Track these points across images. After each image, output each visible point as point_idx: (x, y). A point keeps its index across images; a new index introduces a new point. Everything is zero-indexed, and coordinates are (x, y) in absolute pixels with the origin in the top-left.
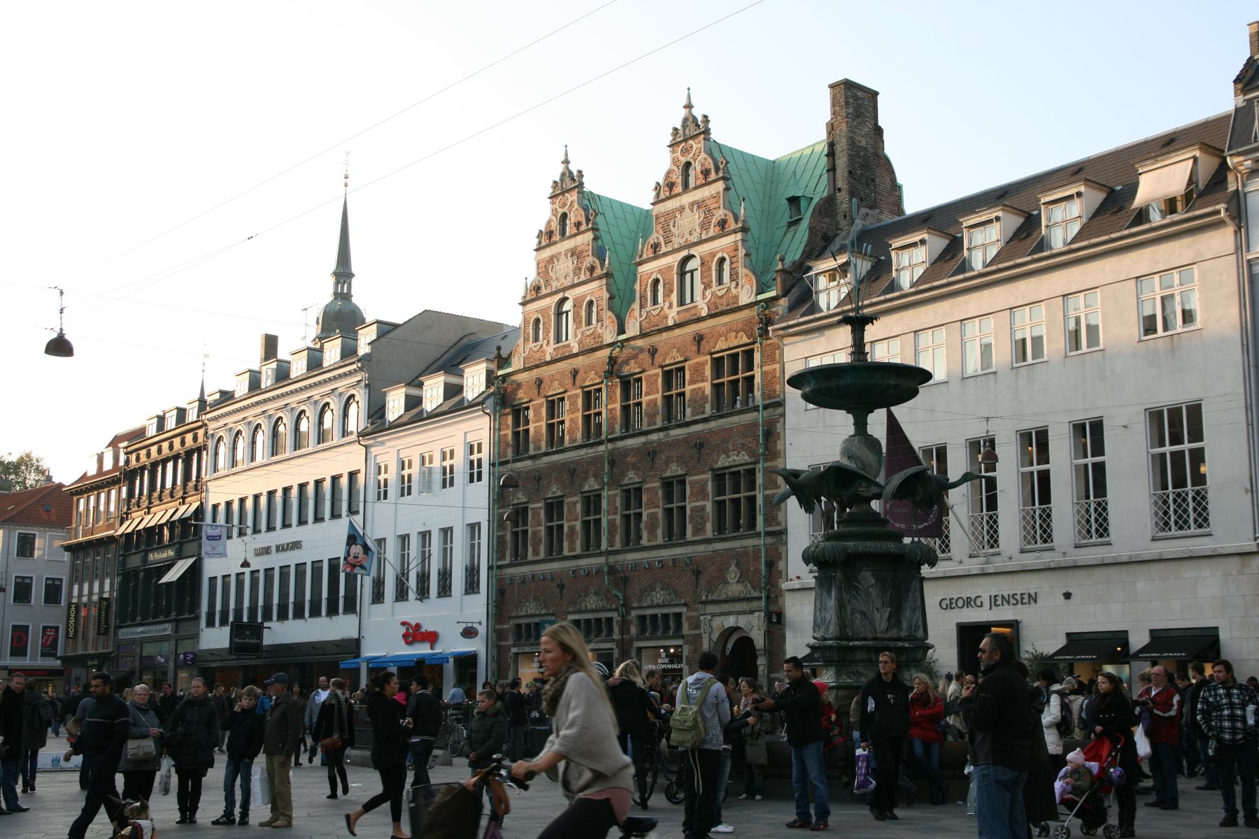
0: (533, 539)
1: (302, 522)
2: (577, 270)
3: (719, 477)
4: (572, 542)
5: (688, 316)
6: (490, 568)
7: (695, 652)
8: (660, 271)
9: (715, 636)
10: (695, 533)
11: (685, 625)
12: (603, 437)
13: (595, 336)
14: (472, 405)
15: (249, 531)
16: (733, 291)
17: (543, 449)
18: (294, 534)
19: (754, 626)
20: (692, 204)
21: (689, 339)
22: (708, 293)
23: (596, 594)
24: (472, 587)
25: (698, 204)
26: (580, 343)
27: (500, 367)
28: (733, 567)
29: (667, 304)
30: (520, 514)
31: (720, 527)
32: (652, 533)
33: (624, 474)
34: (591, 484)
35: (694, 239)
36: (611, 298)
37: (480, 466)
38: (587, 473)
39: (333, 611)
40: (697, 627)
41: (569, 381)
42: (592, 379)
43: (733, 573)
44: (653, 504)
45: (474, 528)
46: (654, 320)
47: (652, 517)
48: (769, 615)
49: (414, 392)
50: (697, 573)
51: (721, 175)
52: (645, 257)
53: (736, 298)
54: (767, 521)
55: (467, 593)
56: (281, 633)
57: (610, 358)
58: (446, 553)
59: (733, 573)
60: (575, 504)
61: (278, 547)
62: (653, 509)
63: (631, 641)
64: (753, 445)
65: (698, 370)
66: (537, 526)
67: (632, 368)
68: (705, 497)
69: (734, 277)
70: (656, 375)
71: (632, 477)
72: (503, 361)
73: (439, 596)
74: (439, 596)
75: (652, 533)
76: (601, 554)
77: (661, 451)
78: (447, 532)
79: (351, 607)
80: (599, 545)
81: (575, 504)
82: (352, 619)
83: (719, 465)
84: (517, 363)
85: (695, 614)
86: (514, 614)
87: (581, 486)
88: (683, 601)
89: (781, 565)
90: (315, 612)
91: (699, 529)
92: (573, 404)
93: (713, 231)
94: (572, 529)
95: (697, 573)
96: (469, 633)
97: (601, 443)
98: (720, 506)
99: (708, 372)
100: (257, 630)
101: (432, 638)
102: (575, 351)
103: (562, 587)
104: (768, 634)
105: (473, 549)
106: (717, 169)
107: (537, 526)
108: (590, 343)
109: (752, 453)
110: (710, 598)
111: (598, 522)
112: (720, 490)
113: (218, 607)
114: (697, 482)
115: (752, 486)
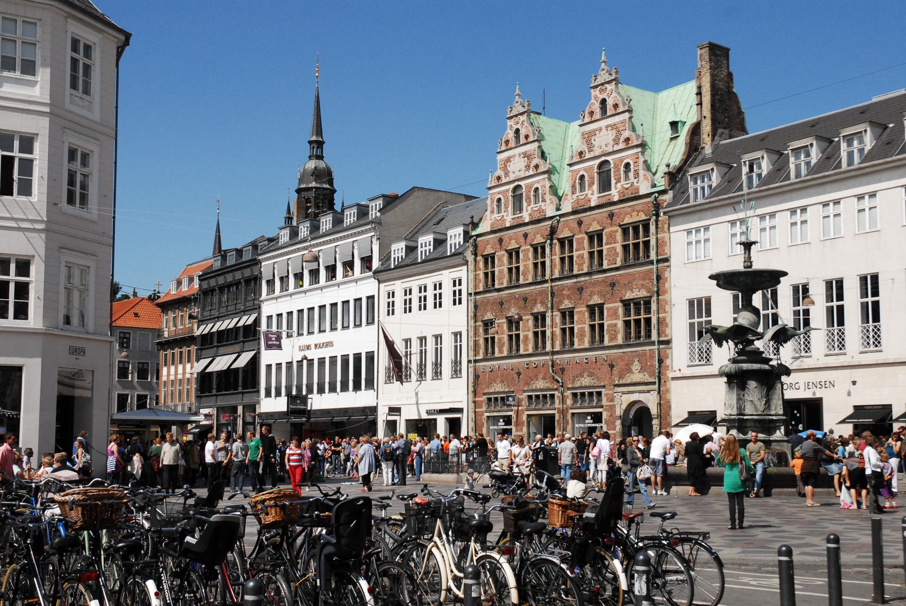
0: (499, 343)
1: (333, 328)
2: (528, 167)
3: (626, 304)
4: (526, 345)
5: (604, 201)
6: (469, 362)
7: (611, 415)
8: (585, 169)
9: (624, 407)
10: (611, 340)
11: (604, 399)
12: (547, 278)
13: (541, 211)
15: (295, 334)
16: (636, 184)
18: (328, 336)
19: (651, 401)
20: (607, 127)
21: (606, 215)
22: (619, 185)
23: (544, 378)
25: (613, 127)
26: (530, 215)
28: (636, 363)
29: (590, 192)
31: (627, 336)
32: (581, 341)
33: (561, 302)
34: (539, 308)
35: (610, 149)
37: (460, 294)
38: (536, 300)
39: (357, 387)
40: (612, 400)
41: (522, 240)
42: (539, 239)
43: (636, 366)
45: (457, 335)
46: (581, 203)
47: (582, 330)
49: (412, 244)
50: (612, 366)
51: (627, 108)
53: (638, 189)
56: (319, 402)
58: (438, 353)
59: (636, 366)
61: (316, 345)
62: (582, 323)
63: (567, 409)
65: (612, 236)
67: (564, 233)
68: (617, 318)
69: (637, 175)
70: (583, 238)
71: (567, 304)
72: (475, 225)
76: (546, 354)
77: (587, 288)
78: (438, 338)
79: (370, 384)
80: (544, 347)
82: (371, 393)
83: (627, 297)
84: (484, 227)
85: (610, 392)
86: (486, 391)
87: (532, 309)
88: (602, 384)
89: (668, 362)
90: (345, 388)
91: (613, 338)
92: (526, 255)
93: (622, 146)
95: (612, 366)
98: (627, 323)
100: (304, 400)
102: (527, 220)
103: (519, 374)
105: (457, 350)
106: (624, 104)
107: (502, 333)
108: (537, 216)
109: (649, 290)
110: (621, 382)
111: (544, 333)
112: (627, 312)
113: (273, 385)
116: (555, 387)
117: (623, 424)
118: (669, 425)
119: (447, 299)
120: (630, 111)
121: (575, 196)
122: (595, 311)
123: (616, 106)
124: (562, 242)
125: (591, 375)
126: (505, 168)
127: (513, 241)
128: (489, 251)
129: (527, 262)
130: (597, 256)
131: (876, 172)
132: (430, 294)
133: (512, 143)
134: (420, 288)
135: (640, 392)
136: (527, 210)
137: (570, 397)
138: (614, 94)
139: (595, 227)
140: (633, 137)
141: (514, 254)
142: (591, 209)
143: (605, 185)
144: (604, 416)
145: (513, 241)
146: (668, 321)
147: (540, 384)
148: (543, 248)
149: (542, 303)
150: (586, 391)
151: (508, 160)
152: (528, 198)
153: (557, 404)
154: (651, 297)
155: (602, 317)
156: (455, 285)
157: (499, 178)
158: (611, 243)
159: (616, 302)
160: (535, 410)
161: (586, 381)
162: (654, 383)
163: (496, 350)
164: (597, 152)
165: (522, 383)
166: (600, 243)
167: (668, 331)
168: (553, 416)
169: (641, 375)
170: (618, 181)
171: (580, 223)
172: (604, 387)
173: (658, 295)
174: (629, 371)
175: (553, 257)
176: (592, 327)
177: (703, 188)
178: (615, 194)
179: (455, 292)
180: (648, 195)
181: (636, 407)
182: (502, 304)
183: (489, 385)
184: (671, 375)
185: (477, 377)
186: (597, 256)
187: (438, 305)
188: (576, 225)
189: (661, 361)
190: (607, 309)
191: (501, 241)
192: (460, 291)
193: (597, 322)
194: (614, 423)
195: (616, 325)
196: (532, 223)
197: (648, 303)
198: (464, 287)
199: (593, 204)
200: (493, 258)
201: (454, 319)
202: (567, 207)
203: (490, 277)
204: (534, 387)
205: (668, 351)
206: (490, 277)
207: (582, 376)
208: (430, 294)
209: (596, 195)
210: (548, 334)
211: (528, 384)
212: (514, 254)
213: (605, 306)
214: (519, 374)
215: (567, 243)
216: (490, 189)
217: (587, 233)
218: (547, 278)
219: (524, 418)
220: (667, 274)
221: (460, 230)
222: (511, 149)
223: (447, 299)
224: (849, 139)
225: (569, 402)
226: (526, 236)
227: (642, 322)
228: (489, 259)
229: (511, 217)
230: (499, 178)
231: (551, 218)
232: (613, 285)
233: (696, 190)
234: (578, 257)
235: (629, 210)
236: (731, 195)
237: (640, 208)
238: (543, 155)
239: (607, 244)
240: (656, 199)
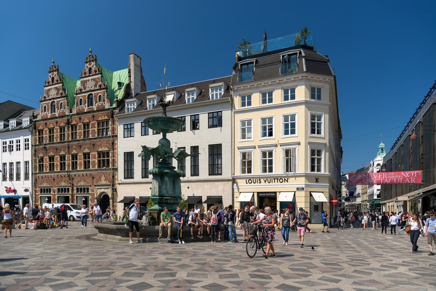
3: (99, 153)
4: (57, 168)
5: (90, 110)
6: (32, 174)
8: (82, 96)
9: (98, 194)
10: (93, 167)
13: (63, 113)
14: (25, 128)
17: (48, 142)
19: (109, 192)
20: (92, 79)
21: (91, 116)
24: (26, 178)
25: (94, 80)
26: (59, 114)
27: (34, 119)
28: (103, 177)
29: (84, 106)
30: (42, 160)
31: (99, 166)
32: (80, 167)
34: (62, 153)
35: (93, 89)
36: (68, 103)
37: (28, 145)
38: (61, 150)
40: (93, 191)
41: (55, 124)
42: (62, 124)
43: (103, 178)
44: (81, 159)
45: (27, 163)
46: (81, 110)
47: (80, 162)
48: (113, 189)
49: (6, 123)
50: (93, 178)
52: (78, 92)
53: (104, 106)
54: (113, 165)
55: (25, 180)
57: (68, 119)
58: (18, 169)
59: (103, 178)
60: (58, 158)
62: (80, 161)
64: (109, 146)
66: (46, 163)
67: (74, 123)
68: (95, 158)
70: (81, 125)
71: (74, 152)
72: (35, 117)
73: (17, 180)
74: (17, 180)
75: (80, 167)
78: (18, 163)
81: (58, 158)
83: (99, 150)
84: (39, 118)
89: (116, 177)
91: (94, 166)
92: (57, 131)
93: (98, 88)
94: (57, 164)
95: (93, 178)
96: (26, 190)
97: (65, 142)
98: (99, 161)
99: (96, 125)
101: (15, 191)
102: (57, 116)
103: (54, 179)
104: (113, 194)
106: (99, 71)
107: (46, 163)
108: (61, 114)
109: (108, 148)
111: (65, 163)
112: (99, 157)
114: (93, 154)
115: (108, 156)
117: (97, 200)
118: (116, 202)
119: (22, 147)
120: (101, 74)
121: (78, 107)
122: (86, 156)
123: (57, 81)
125: (84, 181)
126: (47, 93)
127: (51, 125)
128: (41, 128)
129: (57, 134)
130: (86, 133)
131: (221, 103)
132: (15, 145)
133: (51, 83)
134: (17, 141)
135: (105, 189)
136: (95, 105)
138: (95, 66)
140: (63, 93)
141: (51, 130)
142: (85, 113)
143: (90, 103)
145: (51, 125)
146: (116, 161)
147: (63, 184)
148: (64, 128)
151: (49, 90)
152: (58, 107)
153: (70, 193)
154: (110, 151)
155: (89, 158)
156: (26, 141)
157: (45, 97)
161: (82, 183)
162: (110, 185)
163: (44, 169)
164: (88, 89)
165: (55, 184)
166: (88, 128)
167: (116, 164)
168: (69, 197)
170: (96, 102)
171: (80, 119)
173: (113, 150)
174: (101, 180)
175: (68, 132)
177: (217, 94)
178: (95, 108)
179: (26, 144)
180: (108, 109)
181: (104, 194)
182: (57, 149)
183: (41, 184)
184: (117, 182)
185: (36, 180)
186: (86, 133)
187: (18, 149)
188: (79, 120)
191: (46, 124)
192: (28, 144)
194: (94, 201)
195: (95, 161)
196: (97, 111)
197: (108, 153)
198: (30, 143)
199: (85, 111)
200: (76, 126)
201: (24, 156)
202: (74, 112)
203: (41, 139)
205: (116, 173)
206: (41, 139)
208: (15, 145)
209: (87, 108)
211: (57, 184)
212: (51, 130)
214: (54, 179)
215: (74, 127)
216: (41, 101)
217: (83, 123)
219: (56, 197)
220: (116, 142)
221: (28, 119)
222: (50, 85)
223: (22, 147)
224: (213, 89)
225: (75, 191)
226: (57, 123)
227: (105, 160)
228: (41, 132)
229: (87, 108)
230: (45, 97)
231: (68, 116)
232: (94, 145)
233: (213, 95)
235: (101, 115)
236: (206, 101)
237: (105, 114)
238: (64, 90)
240: (112, 111)
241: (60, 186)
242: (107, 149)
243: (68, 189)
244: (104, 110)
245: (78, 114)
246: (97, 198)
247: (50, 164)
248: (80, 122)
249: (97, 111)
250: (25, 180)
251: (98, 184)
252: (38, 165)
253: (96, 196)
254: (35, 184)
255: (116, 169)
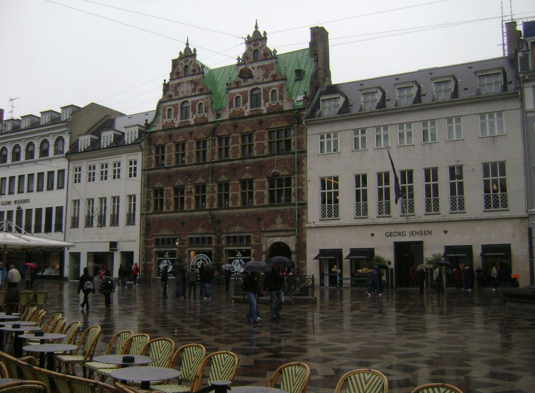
5: (255, 113)
6: (142, 214)
10: (258, 202)
19: (291, 242)
23: (203, 227)
24: (130, 221)
28: (279, 217)
29: (244, 107)
30: (159, 192)
42: (202, 136)
43: (279, 220)
50: (259, 219)
59: (279, 220)
63: (222, 247)
70: (238, 136)
76: (206, 210)
79: (59, 228)
85: (258, 236)
88: (251, 231)
89: (304, 217)
91: (260, 200)
109: (289, 171)
110: (266, 230)
112: (271, 185)
114: (260, 182)
116: (213, 232)
121: (232, 110)
124: (220, 139)
137: (225, 239)
139: (247, 129)
142: (245, 117)
144: (253, 251)
146: (304, 191)
149: (203, 177)
150: (238, 235)
153: (214, 244)
158: (260, 140)
159: (263, 178)
160: (195, 247)
167: (304, 197)
169: (283, 226)
171: (235, 126)
172: (253, 232)
176: (243, 194)
189: (299, 217)
190: (256, 182)
193: (248, 190)
202: (225, 116)
204: (195, 232)
207: (236, 226)
210: (208, 196)
213: (255, 180)
214: (183, 223)
218: (208, 161)
225: (224, 242)
234: (233, 148)
235: (275, 119)
239: (256, 140)
241: (194, 234)
242: (287, 173)
243: (210, 239)
244: (281, 111)
245: (230, 119)
246: (266, 253)
247: (176, 199)
248: (236, 132)
249: (268, 114)
250: (127, 225)
251: (269, 229)
252: (152, 201)
253: (264, 249)
254: (148, 229)
255: (304, 205)
